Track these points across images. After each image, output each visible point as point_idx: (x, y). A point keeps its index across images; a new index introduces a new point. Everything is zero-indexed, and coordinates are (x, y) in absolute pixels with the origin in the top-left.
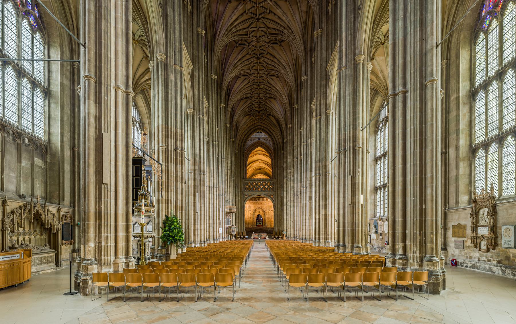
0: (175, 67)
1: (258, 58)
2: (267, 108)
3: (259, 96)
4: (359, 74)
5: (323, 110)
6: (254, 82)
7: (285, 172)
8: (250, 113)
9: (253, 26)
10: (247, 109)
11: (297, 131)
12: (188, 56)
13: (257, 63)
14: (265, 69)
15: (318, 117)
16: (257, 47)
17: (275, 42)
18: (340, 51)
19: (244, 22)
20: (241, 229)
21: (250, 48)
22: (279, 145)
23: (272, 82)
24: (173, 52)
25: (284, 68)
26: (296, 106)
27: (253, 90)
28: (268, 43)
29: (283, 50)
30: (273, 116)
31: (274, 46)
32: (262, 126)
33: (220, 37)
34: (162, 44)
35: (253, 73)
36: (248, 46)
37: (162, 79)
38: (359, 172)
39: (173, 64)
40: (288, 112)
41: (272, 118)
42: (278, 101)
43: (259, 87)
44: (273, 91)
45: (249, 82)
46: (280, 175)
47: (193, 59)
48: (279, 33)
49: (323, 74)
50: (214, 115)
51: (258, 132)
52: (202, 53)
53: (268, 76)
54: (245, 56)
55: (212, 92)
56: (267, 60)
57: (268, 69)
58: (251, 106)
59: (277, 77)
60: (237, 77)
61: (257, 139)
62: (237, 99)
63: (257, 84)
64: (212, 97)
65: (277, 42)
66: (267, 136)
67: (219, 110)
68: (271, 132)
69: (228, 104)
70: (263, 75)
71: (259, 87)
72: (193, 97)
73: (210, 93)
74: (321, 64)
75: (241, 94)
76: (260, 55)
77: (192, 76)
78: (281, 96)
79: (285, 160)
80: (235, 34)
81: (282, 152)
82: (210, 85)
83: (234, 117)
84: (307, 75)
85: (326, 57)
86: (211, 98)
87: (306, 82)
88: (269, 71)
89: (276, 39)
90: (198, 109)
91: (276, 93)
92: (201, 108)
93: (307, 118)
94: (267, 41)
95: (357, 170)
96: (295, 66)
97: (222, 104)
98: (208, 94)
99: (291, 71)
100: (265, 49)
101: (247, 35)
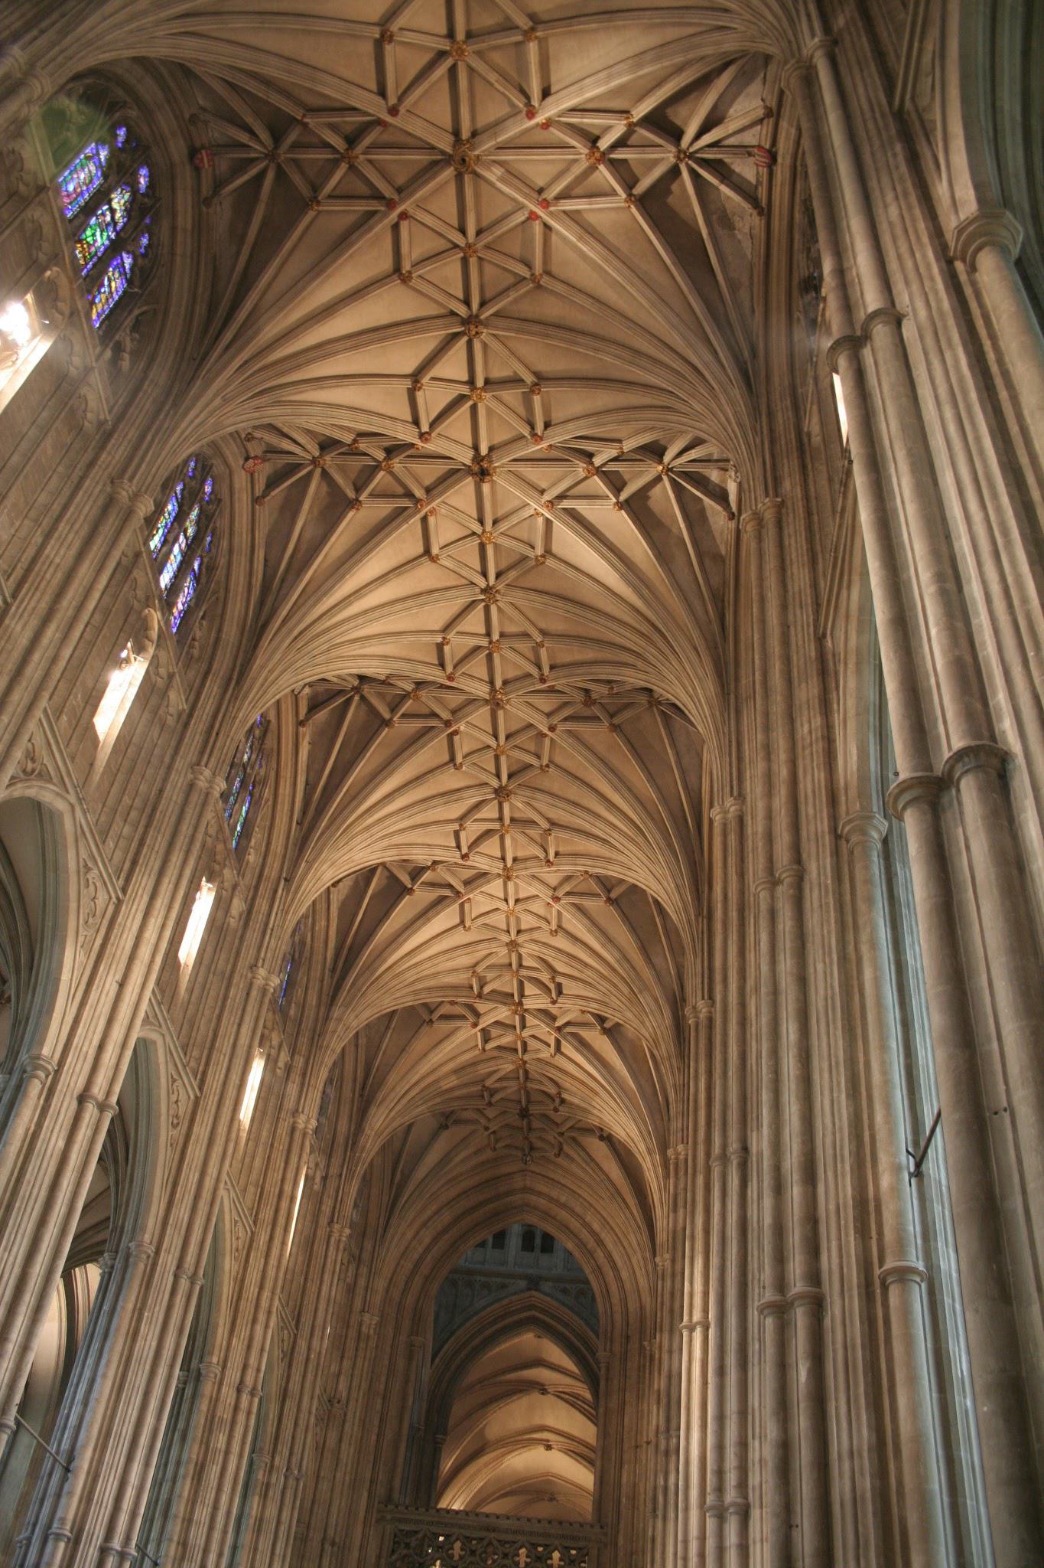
2: (566, 1082)
10: (453, 1081)
17: (587, 712)
22: (633, 1306)
28: (548, 715)
30: (602, 1138)
31: (584, 729)
36: (448, 724)
49: (804, 649)
53: (560, 893)
61: (523, 1284)
63: (505, 938)
67: (236, 993)
69: (327, 1019)
83: (372, 1110)
84: (741, 797)
87: (733, 826)
94: (547, 709)
98: (141, 843)
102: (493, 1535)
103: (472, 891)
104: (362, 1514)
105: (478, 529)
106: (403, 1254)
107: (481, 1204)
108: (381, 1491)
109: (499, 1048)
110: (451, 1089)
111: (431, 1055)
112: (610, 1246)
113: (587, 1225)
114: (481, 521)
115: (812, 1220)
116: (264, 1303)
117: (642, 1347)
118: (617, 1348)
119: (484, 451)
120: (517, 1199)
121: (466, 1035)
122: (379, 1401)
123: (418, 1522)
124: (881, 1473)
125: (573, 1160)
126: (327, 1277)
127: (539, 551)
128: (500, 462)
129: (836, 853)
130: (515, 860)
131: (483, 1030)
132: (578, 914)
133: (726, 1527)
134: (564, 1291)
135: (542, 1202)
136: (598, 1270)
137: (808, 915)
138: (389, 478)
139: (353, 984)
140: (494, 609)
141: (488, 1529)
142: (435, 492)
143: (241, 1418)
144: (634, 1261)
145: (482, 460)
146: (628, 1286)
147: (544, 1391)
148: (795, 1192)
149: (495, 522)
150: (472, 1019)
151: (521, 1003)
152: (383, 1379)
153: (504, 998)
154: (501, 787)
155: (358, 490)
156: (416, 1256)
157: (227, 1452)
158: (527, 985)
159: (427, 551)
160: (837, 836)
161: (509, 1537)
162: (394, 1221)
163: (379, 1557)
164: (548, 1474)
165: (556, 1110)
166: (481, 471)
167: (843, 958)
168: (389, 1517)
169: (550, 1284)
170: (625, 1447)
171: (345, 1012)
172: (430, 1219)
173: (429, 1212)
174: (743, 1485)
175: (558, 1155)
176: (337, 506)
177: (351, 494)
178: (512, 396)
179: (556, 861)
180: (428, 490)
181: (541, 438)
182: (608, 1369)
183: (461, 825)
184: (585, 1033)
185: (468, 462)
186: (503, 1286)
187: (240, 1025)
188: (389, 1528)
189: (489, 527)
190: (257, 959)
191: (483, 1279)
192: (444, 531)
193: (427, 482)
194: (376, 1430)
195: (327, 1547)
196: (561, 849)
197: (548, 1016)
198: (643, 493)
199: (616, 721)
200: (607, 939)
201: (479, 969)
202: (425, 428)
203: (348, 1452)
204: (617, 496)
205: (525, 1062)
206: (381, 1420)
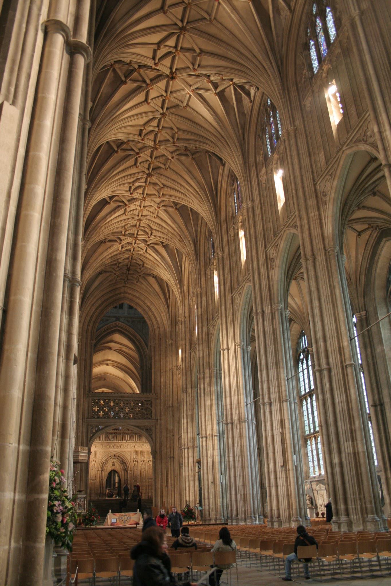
6: (133, 214)
10: (110, 261)
17: (185, 153)
21: (140, 157)
28: (172, 153)
30: (153, 277)
31: (183, 158)
36: (137, 154)
51: (116, 307)
53: (160, 206)
58: (116, 255)
61: (114, 319)
63: (137, 218)
65: (188, 153)
74: (302, 176)
81: (169, 342)
84: (253, 201)
87: (251, 210)
94: (171, 149)
102: (123, 399)
103: (131, 204)
105: (164, 94)
106: (87, 314)
107: (110, 297)
108: (87, 388)
109: (127, 250)
110: (108, 263)
111: (105, 253)
112: (153, 310)
113: (145, 304)
114: (166, 91)
115: (326, 351)
117: (166, 342)
118: (157, 342)
119: (174, 70)
120: (122, 295)
121: (117, 246)
124: (348, 405)
125: (142, 283)
127: (185, 105)
128: (179, 76)
129: (326, 255)
130: (147, 194)
131: (123, 245)
132: (165, 213)
133: (266, 407)
134: (128, 321)
135: (130, 297)
136: (150, 318)
138: (137, 74)
139: (88, 235)
140: (163, 120)
141: (121, 397)
142: (154, 82)
144: (162, 315)
145: (173, 74)
146: (160, 323)
147: (110, 349)
148: (322, 344)
149: (171, 92)
150: (119, 242)
151: (137, 237)
152: (84, 355)
153: (131, 235)
154: (149, 173)
155: (126, 77)
156: (90, 315)
158: (140, 231)
159: (146, 100)
160: (325, 250)
161: (128, 399)
164: (105, 373)
165: (140, 269)
166: (172, 77)
167: (330, 286)
168: (90, 396)
169: (123, 319)
170: (162, 371)
171: (87, 244)
172: (95, 303)
173: (94, 301)
174: (269, 398)
175: (137, 282)
176: (118, 83)
177: (123, 79)
178: (189, 55)
179: (162, 197)
180: (151, 80)
181: (196, 70)
182: (154, 348)
183: (133, 184)
184: (156, 247)
185: (168, 74)
186: (107, 320)
188: (90, 399)
189: (168, 95)
192: (153, 94)
193: (151, 77)
194: (83, 371)
196: (164, 193)
197: (145, 241)
198: (223, 91)
199: (194, 157)
200: (174, 221)
201: (126, 227)
202: (157, 61)
204: (215, 90)
205: (133, 254)
206: (85, 367)
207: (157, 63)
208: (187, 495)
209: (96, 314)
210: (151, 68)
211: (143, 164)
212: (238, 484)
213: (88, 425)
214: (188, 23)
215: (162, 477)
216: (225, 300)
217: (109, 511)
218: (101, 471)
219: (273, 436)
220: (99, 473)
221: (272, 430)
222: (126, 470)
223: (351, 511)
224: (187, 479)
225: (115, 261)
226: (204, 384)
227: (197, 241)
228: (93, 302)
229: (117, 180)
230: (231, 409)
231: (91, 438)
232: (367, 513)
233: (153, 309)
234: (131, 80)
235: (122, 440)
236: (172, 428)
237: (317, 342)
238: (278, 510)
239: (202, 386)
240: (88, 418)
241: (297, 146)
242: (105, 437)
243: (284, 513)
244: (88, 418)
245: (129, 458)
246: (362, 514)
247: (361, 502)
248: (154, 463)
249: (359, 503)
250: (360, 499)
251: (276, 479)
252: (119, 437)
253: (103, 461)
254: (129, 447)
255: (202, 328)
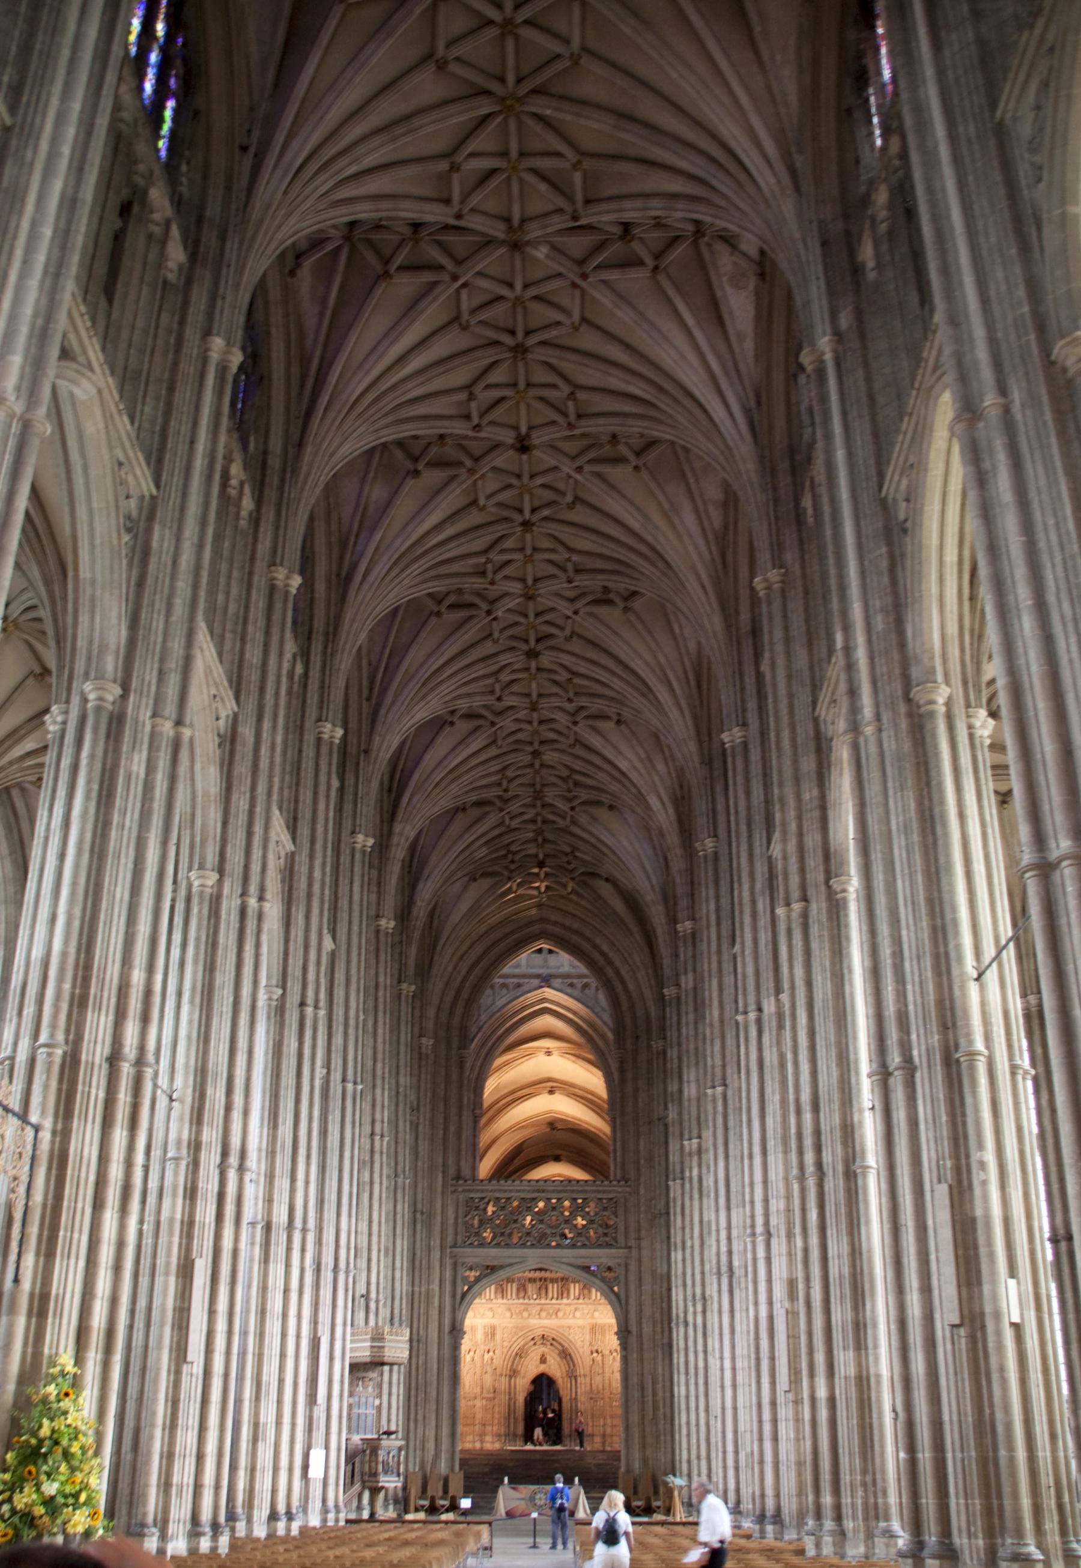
0: (153, 727)
1: (532, 654)
2: (580, 845)
3: (538, 796)
4: (937, 754)
5: (815, 875)
6: (517, 742)
7: (674, 1146)
8: (496, 868)
9: (508, 544)
10: (484, 851)
11: (719, 952)
12: (219, 672)
13: (527, 669)
14: (561, 693)
15: (797, 907)
16: (526, 616)
17: (604, 597)
18: (850, 667)
19: (472, 535)
20: (437, 1456)
21: (495, 619)
23: (596, 741)
24: (155, 673)
25: (645, 690)
26: (709, 843)
27: (510, 773)
28: (572, 600)
29: (639, 625)
30: (607, 880)
31: (602, 611)
32: (555, 923)
33: (366, 586)
34: (113, 646)
35: (512, 707)
36: (489, 613)
37: (90, 771)
38: (982, 1165)
39: (149, 714)
40: (678, 865)
41: (606, 890)
42: (631, 818)
43: (537, 763)
44: (602, 776)
45: (494, 742)
46: (650, 1159)
47: (240, 677)
48: (616, 567)
49: (805, 730)
50: (316, 888)
51: (540, 951)
52: (281, 655)
53: (578, 719)
54: (472, 646)
55: (316, 793)
56: (574, 659)
57: (577, 694)
58: (500, 835)
59: (619, 722)
60: (439, 724)
62: (436, 810)
63: (530, 749)
64: (315, 811)
65: (612, 596)
66: (582, 968)
67: (345, 859)
68: (603, 954)
69: (390, 833)
70: (558, 716)
71: (537, 763)
72: (225, 823)
73: (306, 795)
74: (791, 696)
75: (455, 789)
76: (538, 640)
77: (229, 741)
78: (641, 797)
79: (673, 1087)
80: (433, 573)
81: (657, 1045)
82: (308, 765)
83: (420, 886)
84: (745, 724)
85: (811, 667)
86: (308, 815)
87: (739, 750)
88: (583, 701)
89: (606, 590)
90: (238, 870)
91: (614, 787)
92: (255, 868)
93: (753, 902)
94: (571, 594)
95: (975, 1156)
96: (693, 682)
97: (360, 838)
98: (297, 801)
99: (677, 703)
100: (560, 622)
101: (483, 573)
104: (439, 1189)
108: (452, 1171)
112: (617, 962)
113: (596, 947)
115: (817, 1133)
116: (379, 1072)
117: (649, 1047)
119: (523, 430)
122: (442, 1104)
123: (482, 1191)
124: (853, 1265)
126: (403, 1027)
134: (571, 985)
137: (812, 938)
141: (538, 1191)
143: (377, 1157)
144: (639, 976)
148: (808, 1117)
152: (443, 1087)
155: (416, 460)
157: (372, 1183)
162: (436, 958)
163: (456, 1218)
164: (550, 1112)
172: (466, 952)
173: (464, 948)
174: (767, 1223)
186: (519, 986)
187: (351, 883)
188: (461, 1197)
190: (354, 825)
191: (502, 981)
195: (418, 1216)
199: (629, 604)
203: (424, 1147)
206: (445, 1118)
207: (478, 426)
208: (684, 1445)
209: (472, 978)
210: (466, 437)
211: (510, 632)
212: (741, 1428)
213: (455, 1265)
214: (528, 333)
215: (643, 1396)
216: (720, 963)
217: (502, 1482)
218: (510, 1377)
219: (771, 1318)
220: (504, 1381)
221: (770, 1303)
222: (572, 1375)
223: (847, 1511)
224: (683, 1406)
225: (500, 849)
226: (700, 1166)
227: (683, 798)
228: (460, 952)
229: (450, 677)
230: (729, 1239)
231: (464, 1295)
232: (877, 1518)
233: (617, 961)
234: (431, 465)
235: (561, 1295)
236: (665, 1270)
237: (799, 1112)
238: (777, 1496)
239: (695, 1172)
240: (455, 1246)
241: (785, 617)
242: (518, 1290)
243: (789, 1506)
244: (455, 1246)
245: (579, 1344)
246: (866, 1519)
247: (866, 1491)
248: (625, 1360)
249: (860, 1493)
250: (864, 1484)
251: (775, 1421)
252: (553, 1289)
253: (515, 1349)
254: (578, 1314)
255: (696, 1023)
